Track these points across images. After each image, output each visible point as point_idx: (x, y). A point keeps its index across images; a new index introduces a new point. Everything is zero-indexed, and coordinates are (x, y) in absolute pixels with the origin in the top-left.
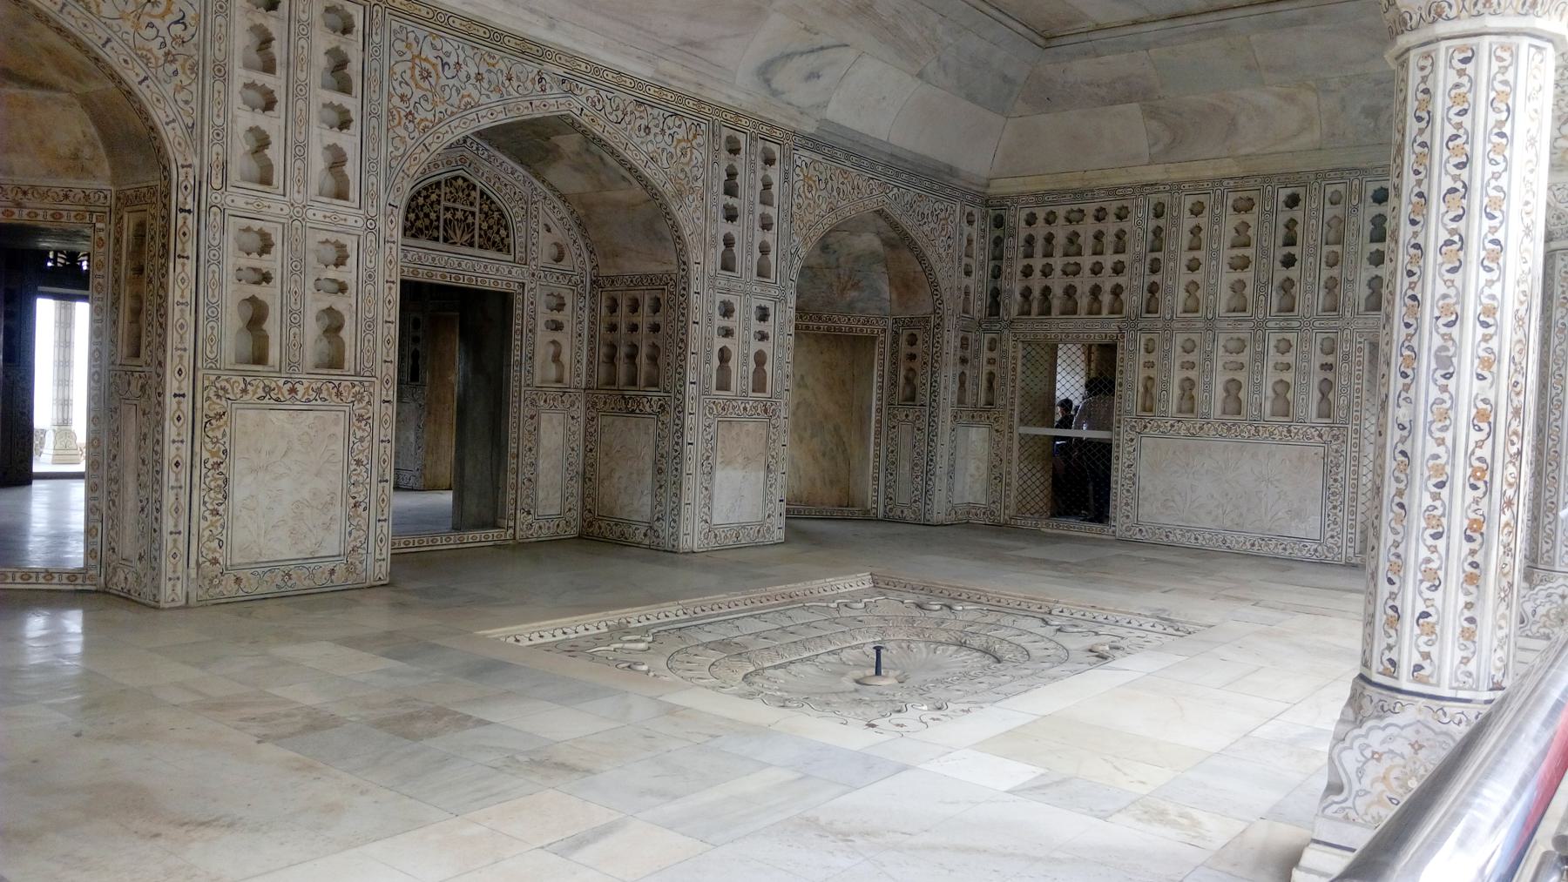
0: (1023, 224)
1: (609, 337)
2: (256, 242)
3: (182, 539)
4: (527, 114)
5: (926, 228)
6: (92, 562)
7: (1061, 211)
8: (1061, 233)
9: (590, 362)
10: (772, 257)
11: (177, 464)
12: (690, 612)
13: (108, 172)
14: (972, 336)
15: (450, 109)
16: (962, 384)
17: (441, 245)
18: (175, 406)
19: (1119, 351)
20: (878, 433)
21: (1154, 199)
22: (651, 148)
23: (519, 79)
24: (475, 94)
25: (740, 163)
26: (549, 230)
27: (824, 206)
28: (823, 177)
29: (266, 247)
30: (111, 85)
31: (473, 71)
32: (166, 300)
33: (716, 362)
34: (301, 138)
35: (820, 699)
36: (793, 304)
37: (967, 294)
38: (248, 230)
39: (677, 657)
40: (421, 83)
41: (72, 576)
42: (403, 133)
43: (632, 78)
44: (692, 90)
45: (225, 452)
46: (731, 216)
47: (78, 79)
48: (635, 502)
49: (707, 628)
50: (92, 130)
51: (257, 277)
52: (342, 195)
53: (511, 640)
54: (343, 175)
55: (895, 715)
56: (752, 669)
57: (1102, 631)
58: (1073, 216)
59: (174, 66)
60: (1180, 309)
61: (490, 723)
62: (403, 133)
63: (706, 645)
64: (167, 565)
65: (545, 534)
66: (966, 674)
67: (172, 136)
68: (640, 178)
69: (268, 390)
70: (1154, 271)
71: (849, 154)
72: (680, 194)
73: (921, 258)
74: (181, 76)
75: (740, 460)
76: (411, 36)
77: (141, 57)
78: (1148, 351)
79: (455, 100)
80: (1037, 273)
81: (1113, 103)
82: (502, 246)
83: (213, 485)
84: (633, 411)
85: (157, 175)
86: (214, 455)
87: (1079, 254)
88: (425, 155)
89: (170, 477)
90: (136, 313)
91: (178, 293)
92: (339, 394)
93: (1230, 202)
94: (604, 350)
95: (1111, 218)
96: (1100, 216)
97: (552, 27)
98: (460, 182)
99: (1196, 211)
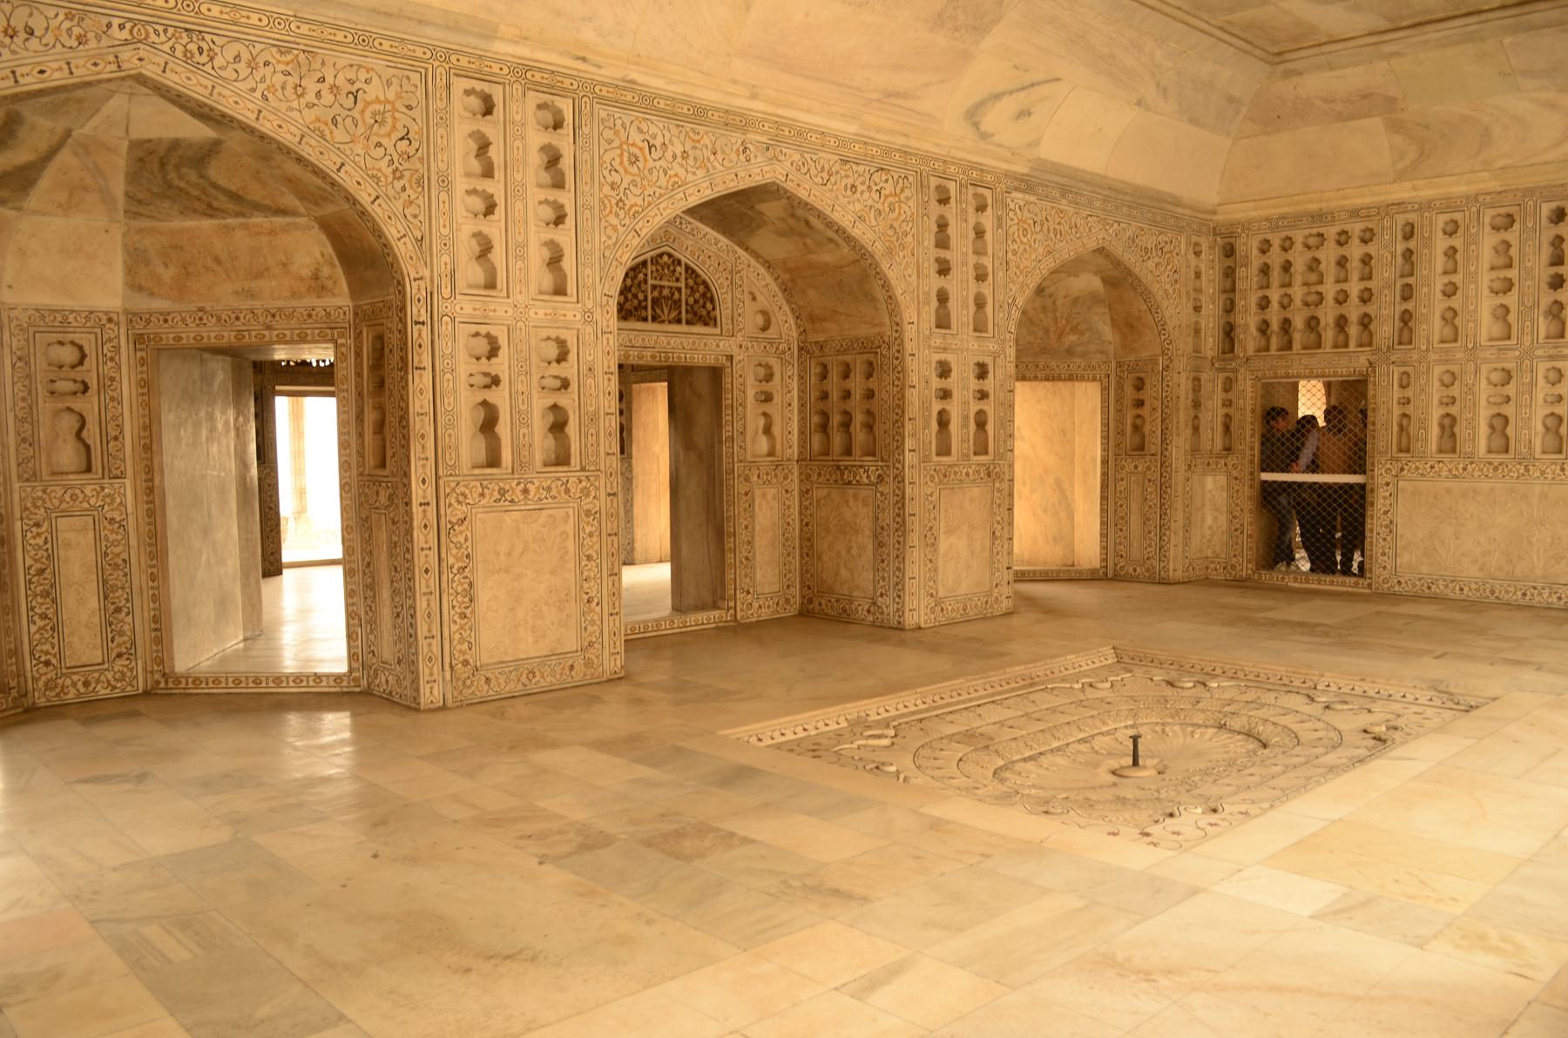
0: (1255, 252)
1: (820, 406)
2: (482, 346)
3: (436, 643)
4: (734, 185)
5: (1150, 264)
6: (355, 665)
7: (1299, 236)
8: (1299, 260)
9: (802, 433)
10: (989, 309)
11: (427, 571)
12: (929, 700)
13: (345, 288)
14: (1204, 377)
15: (658, 191)
16: (1196, 429)
17: (649, 326)
18: (421, 515)
19: (1370, 386)
20: (1105, 486)
21: (1401, 219)
22: (858, 206)
23: (723, 152)
24: (682, 172)
25: (951, 212)
26: (754, 299)
27: (1041, 250)
29: (493, 352)
30: (347, 206)
31: (679, 150)
32: (407, 412)
33: (934, 426)
34: (520, 239)
35: (1084, 803)
36: (1013, 359)
37: (1197, 332)
38: (477, 334)
39: (923, 752)
40: (630, 168)
41: (338, 678)
42: (613, 220)
43: (836, 136)
44: (900, 141)
45: (468, 556)
46: (944, 269)
47: (316, 204)
48: (857, 574)
49: (949, 718)
50: (330, 250)
51: (487, 380)
52: (560, 291)
53: (754, 740)
54: (561, 269)
55: (1169, 821)
56: (1001, 763)
57: (1376, 708)
58: (1312, 241)
59: (402, 183)
60: (1437, 338)
61: (753, 841)
62: (613, 220)
63: (951, 737)
64: (423, 670)
65: (765, 614)
66: (1231, 763)
67: (403, 249)
68: (849, 239)
69: (502, 492)
70: (1405, 299)
71: (1064, 191)
72: (890, 252)
73: (1146, 295)
74: (409, 191)
75: (965, 528)
76: (619, 122)
77: (372, 177)
78: (1403, 387)
79: (663, 181)
80: (1275, 305)
81: (1353, 117)
82: (708, 320)
83: (459, 589)
84: (849, 483)
85: (392, 290)
86: (458, 560)
87: (1321, 282)
88: (636, 241)
89: (421, 584)
90: (380, 427)
91: (417, 404)
92: (567, 491)
93: (1487, 220)
94: (816, 419)
95: (1356, 241)
96: (1343, 239)
97: (754, 97)
98: (665, 258)
99: (1452, 230)
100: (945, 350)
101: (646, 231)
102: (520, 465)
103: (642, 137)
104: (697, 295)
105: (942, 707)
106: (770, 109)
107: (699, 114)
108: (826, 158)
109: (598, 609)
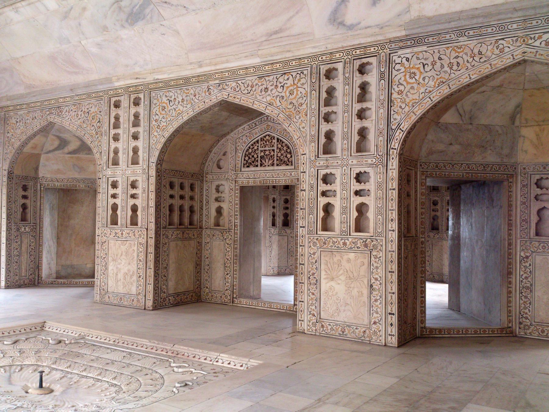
17: (259, 168)
22: (269, 98)
23: (199, 94)
24: (181, 108)
25: (338, 83)
27: (432, 83)
28: (429, 62)
34: (125, 147)
42: (156, 134)
43: (254, 67)
44: (289, 55)
62: (156, 134)
69: (116, 233)
71: (461, 32)
72: (289, 117)
74: (99, 138)
75: (343, 278)
76: (159, 96)
88: (163, 140)
92: (134, 235)
97: (201, 66)
98: (267, 137)
100: (327, 167)
101: (167, 135)
102: (122, 225)
103: (167, 98)
104: (283, 152)
105: (119, 346)
106: (213, 68)
107: (187, 81)
108: (250, 80)
109: (142, 280)
